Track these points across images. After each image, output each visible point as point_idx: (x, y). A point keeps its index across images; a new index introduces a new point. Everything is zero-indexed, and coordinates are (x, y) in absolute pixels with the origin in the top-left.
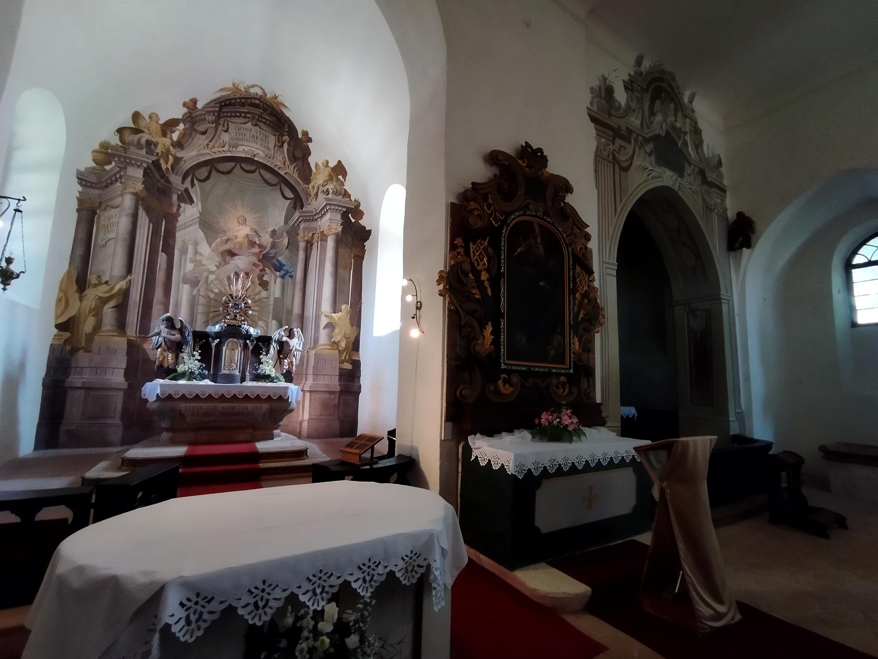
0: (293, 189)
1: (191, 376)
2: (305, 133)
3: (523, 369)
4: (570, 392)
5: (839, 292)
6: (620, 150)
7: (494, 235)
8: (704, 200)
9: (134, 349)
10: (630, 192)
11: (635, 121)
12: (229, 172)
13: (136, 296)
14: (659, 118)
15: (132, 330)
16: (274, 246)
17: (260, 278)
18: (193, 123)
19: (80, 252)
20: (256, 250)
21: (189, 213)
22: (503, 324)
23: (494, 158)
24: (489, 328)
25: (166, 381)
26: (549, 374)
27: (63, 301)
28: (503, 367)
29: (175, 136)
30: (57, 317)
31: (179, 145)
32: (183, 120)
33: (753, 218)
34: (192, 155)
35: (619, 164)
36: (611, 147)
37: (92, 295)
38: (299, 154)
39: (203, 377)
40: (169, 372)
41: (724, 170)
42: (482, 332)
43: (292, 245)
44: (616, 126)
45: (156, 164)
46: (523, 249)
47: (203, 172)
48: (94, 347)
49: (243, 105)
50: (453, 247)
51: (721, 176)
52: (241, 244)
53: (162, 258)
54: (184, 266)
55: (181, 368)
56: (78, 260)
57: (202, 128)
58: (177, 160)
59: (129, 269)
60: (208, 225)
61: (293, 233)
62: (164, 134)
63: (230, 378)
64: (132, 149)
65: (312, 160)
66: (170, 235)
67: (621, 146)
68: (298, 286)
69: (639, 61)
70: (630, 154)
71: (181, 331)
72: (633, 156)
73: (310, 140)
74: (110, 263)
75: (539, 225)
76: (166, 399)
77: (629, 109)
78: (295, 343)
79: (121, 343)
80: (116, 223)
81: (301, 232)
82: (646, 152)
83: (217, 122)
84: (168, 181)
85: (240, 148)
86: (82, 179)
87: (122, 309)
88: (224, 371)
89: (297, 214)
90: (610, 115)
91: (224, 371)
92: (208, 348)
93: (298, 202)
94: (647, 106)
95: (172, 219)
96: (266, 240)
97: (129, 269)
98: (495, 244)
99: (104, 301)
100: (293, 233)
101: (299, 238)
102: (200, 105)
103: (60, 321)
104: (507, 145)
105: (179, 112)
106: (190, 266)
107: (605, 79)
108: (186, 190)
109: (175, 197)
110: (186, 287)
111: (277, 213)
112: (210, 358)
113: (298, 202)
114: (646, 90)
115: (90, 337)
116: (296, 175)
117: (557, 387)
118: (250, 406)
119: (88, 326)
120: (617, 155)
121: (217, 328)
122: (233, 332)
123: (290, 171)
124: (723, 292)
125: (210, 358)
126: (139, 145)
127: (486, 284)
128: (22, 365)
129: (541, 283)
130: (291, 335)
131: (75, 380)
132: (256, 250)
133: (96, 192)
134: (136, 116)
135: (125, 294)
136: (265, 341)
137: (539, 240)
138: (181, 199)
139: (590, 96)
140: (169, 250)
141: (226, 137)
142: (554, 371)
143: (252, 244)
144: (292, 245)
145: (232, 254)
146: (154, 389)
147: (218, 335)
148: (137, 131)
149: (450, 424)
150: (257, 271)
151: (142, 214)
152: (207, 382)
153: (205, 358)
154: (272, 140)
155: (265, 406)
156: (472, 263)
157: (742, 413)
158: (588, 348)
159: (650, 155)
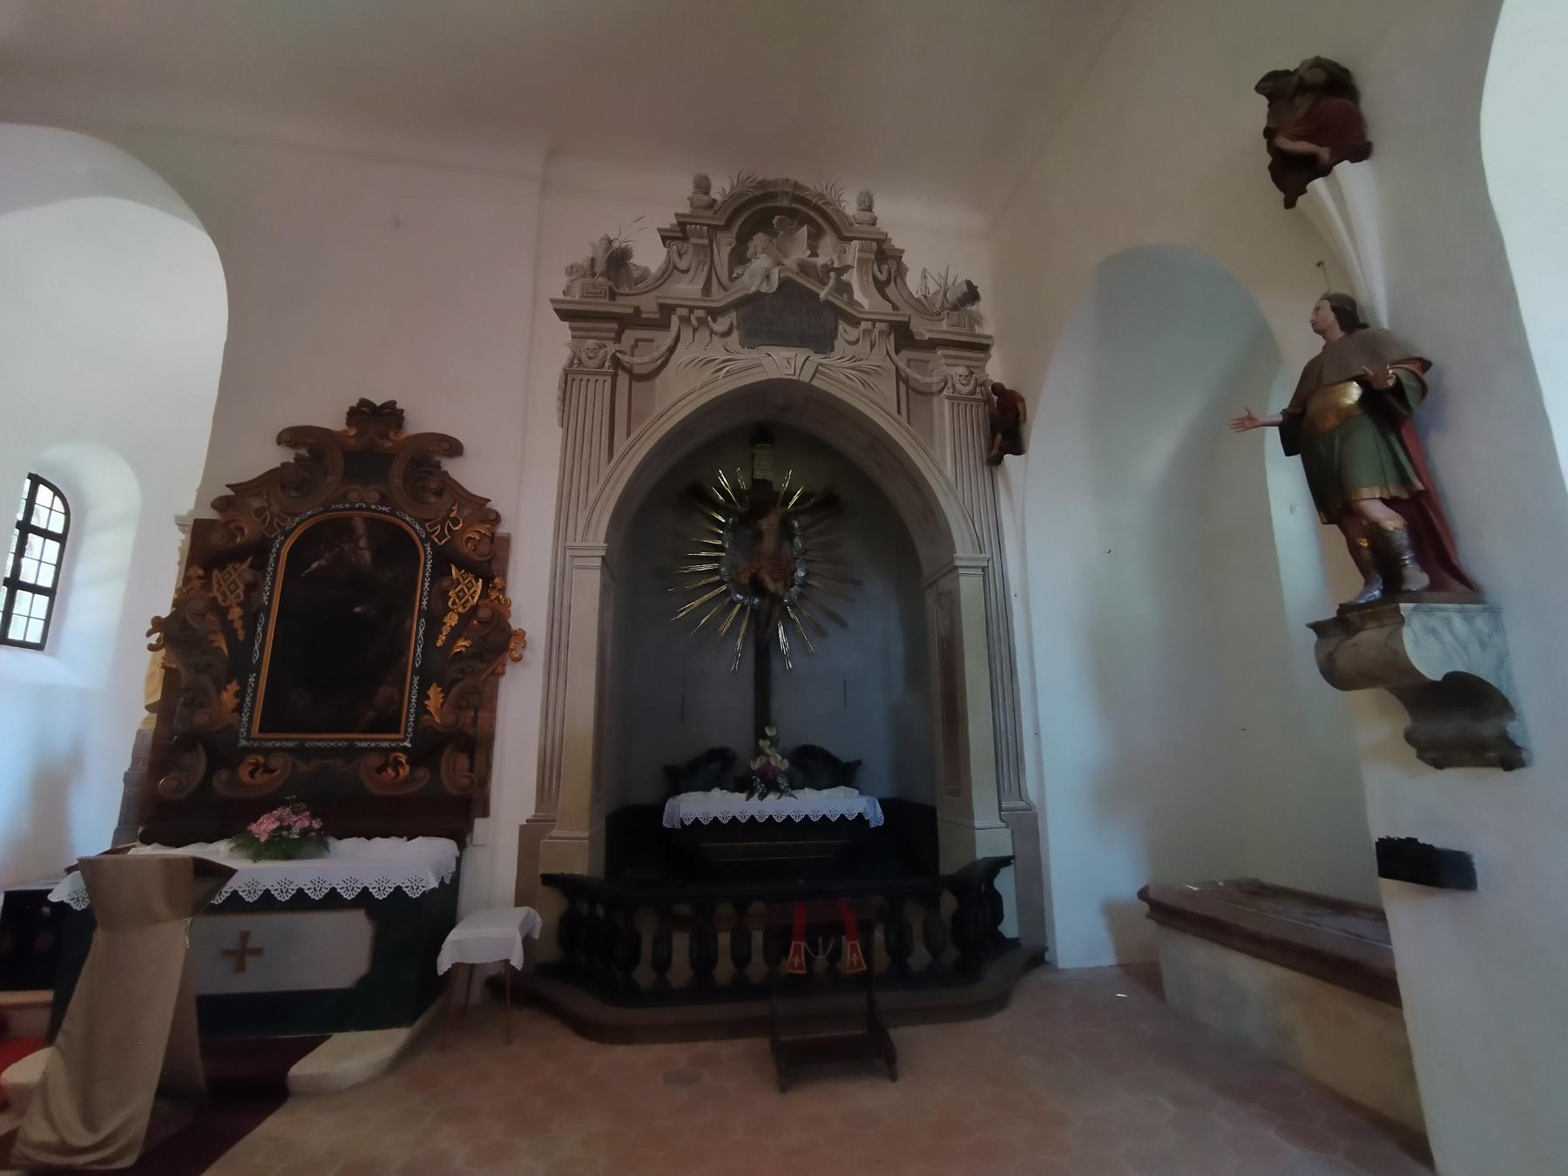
3: (291, 744)
4: (411, 778)
6: (635, 347)
7: (258, 552)
8: (900, 377)
10: (658, 410)
11: (687, 289)
14: (761, 262)
23: (292, 437)
24: (234, 687)
26: (352, 753)
28: (243, 743)
30: (148, 697)
33: (1024, 393)
35: (630, 372)
36: (611, 348)
41: (983, 307)
42: (219, 694)
44: (631, 311)
46: (323, 562)
51: (975, 320)
67: (637, 340)
69: (703, 185)
70: (664, 348)
72: (672, 349)
77: (670, 271)
82: (712, 332)
90: (613, 295)
94: (722, 255)
98: (260, 566)
103: (152, 701)
104: (328, 413)
107: (610, 242)
114: (727, 226)
117: (381, 769)
120: (625, 358)
124: (963, 550)
127: (238, 625)
129: (357, 610)
137: (362, 543)
142: (364, 744)
156: (215, 599)
157: (1030, 808)
158: (479, 702)
159: (728, 333)
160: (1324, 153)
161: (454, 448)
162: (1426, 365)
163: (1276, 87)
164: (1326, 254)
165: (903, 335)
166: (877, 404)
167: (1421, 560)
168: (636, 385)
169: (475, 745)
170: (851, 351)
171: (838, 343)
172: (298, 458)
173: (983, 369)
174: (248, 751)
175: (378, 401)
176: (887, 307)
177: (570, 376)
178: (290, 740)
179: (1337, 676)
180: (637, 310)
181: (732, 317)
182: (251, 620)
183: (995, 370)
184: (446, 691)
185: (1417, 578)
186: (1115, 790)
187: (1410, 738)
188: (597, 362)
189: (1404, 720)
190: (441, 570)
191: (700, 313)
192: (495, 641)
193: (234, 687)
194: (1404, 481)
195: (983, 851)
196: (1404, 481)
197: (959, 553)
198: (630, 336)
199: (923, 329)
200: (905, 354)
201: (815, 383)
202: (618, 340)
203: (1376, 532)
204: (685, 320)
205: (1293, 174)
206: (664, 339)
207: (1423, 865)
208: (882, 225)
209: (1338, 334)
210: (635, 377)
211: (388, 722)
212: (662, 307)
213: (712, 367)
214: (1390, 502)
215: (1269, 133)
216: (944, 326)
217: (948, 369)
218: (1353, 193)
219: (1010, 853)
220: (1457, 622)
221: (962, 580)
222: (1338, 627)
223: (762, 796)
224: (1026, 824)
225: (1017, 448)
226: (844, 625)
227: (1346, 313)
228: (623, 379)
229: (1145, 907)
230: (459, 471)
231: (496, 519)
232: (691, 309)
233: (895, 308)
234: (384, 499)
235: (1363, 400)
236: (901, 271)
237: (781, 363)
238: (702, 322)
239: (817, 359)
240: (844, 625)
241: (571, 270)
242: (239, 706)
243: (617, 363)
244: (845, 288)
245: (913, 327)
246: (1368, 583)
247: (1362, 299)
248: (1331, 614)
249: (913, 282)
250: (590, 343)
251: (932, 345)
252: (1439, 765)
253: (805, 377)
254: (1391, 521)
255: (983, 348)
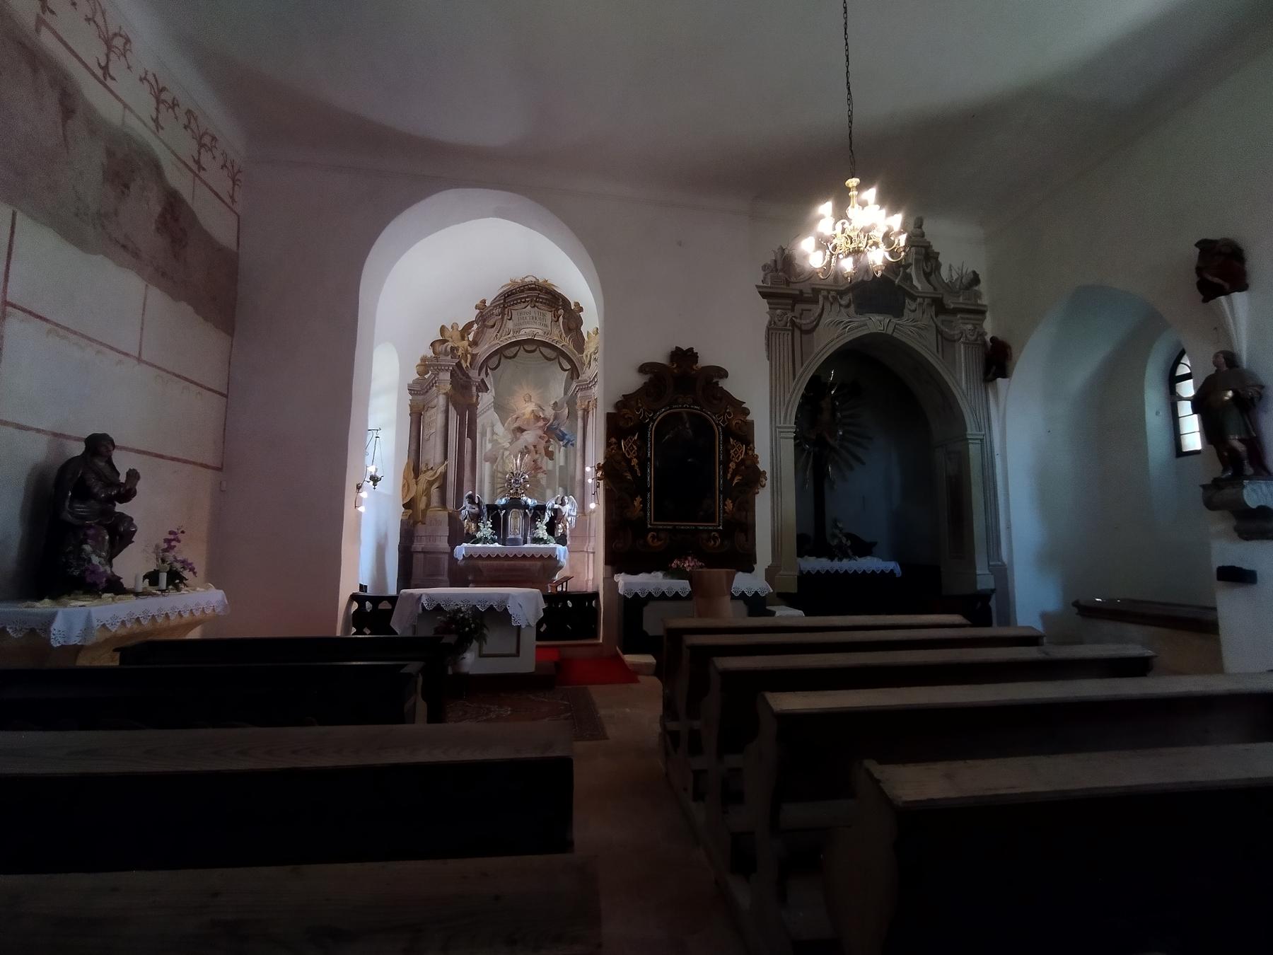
0: (570, 361)
1: (485, 540)
2: (577, 304)
5: (1157, 413)
7: (642, 428)
8: (939, 332)
9: (453, 520)
10: (816, 350)
12: (515, 355)
13: (451, 477)
15: (451, 506)
16: (556, 417)
17: (546, 449)
18: (484, 321)
19: (413, 447)
20: (541, 423)
21: (486, 399)
22: (651, 496)
24: (639, 499)
25: (469, 545)
27: (406, 487)
29: (471, 337)
31: (474, 343)
32: (476, 321)
34: (483, 350)
35: (800, 329)
36: (790, 315)
37: (424, 478)
38: (573, 325)
39: (494, 541)
40: (471, 538)
41: (982, 287)
43: (572, 415)
45: (459, 365)
47: (495, 359)
48: (428, 521)
49: (522, 291)
50: (608, 444)
51: (978, 295)
52: (528, 420)
53: (468, 442)
54: (485, 446)
55: (479, 535)
56: (413, 453)
57: (491, 323)
58: (474, 356)
59: (446, 458)
60: (501, 408)
61: (571, 403)
62: (463, 338)
63: (515, 542)
64: (442, 357)
65: (584, 329)
66: (473, 422)
68: (579, 454)
71: (479, 505)
72: (821, 315)
73: (581, 309)
74: (432, 453)
75: (688, 413)
76: (469, 558)
78: (567, 509)
79: (444, 516)
80: (435, 419)
81: (578, 402)
83: (502, 314)
84: (468, 377)
85: (522, 332)
86: (412, 390)
87: (443, 489)
88: (510, 536)
89: (574, 385)
91: (510, 536)
92: (497, 516)
93: (574, 372)
95: (472, 408)
96: (549, 413)
97: (446, 458)
98: (643, 438)
99: (431, 483)
100: (571, 403)
101: (577, 407)
102: (488, 304)
105: (472, 315)
106: (489, 446)
108: (483, 380)
109: (474, 389)
110: (487, 465)
111: (557, 387)
112: (499, 526)
113: (574, 372)
115: (424, 512)
116: (571, 346)
118: (527, 563)
119: (422, 505)
121: (503, 501)
122: (515, 503)
123: (565, 343)
124: (971, 430)
125: (499, 526)
126: (446, 354)
127: (636, 468)
128: (386, 535)
130: (563, 504)
131: (418, 546)
132: (541, 423)
133: (421, 397)
134: (443, 329)
135: (444, 476)
136: (540, 510)
138: (479, 390)
139: (762, 273)
140: (472, 435)
141: (510, 325)
143: (538, 418)
144: (572, 415)
145: (521, 430)
146: (462, 550)
147: (504, 507)
148: (444, 341)
149: (609, 568)
150: (543, 443)
151: (451, 407)
152: (497, 545)
153: (495, 527)
154: (549, 316)
155: (539, 563)
157: (1004, 565)
158: (747, 507)
159: (848, 306)
160: (1227, 286)
161: (722, 373)
162: (1262, 387)
163: (1206, 247)
164: (1220, 328)
165: (939, 306)
166: (926, 347)
167: (1251, 463)
168: (805, 337)
169: (747, 529)
170: (912, 315)
171: (906, 311)
172: (651, 380)
173: (981, 326)
174: (651, 530)
175: (685, 348)
176: (930, 289)
177: (771, 330)
178: (669, 525)
179: (1210, 505)
180: (801, 291)
181: (850, 296)
182: (643, 463)
183: (990, 328)
184: (733, 503)
185: (1249, 470)
186: (1050, 557)
187: (1236, 529)
188: (783, 323)
189: (1233, 522)
190: (726, 441)
191: (833, 293)
192: (752, 478)
193: (639, 499)
194: (1248, 432)
195: (980, 587)
196: (1248, 432)
197: (969, 432)
198: (798, 307)
199: (950, 303)
200: (942, 317)
201: (895, 335)
202: (793, 310)
203: (1233, 451)
204: (826, 298)
205: (1209, 291)
206: (816, 310)
207: (1237, 576)
208: (927, 238)
209: (1225, 368)
210: (803, 332)
211: (710, 517)
212: (814, 290)
213: (841, 326)
214: (1240, 440)
215: (1199, 270)
216: (961, 300)
217: (964, 326)
218: (1239, 306)
219: (992, 587)
220: (1264, 487)
221: (971, 446)
222: (1217, 484)
223: (840, 560)
224: (1002, 573)
225: (1003, 372)
226: (863, 463)
227: (1230, 359)
228: (797, 333)
229: (1076, 610)
230: (727, 385)
231: (746, 412)
232: (829, 291)
233: (935, 289)
234: (695, 402)
235: (1233, 399)
236: (938, 266)
237: (876, 323)
238: (835, 298)
239: (894, 320)
240: (863, 463)
241: (765, 267)
242: (643, 506)
243: (793, 323)
244: (908, 277)
245: (945, 301)
246: (1225, 470)
247: (1236, 350)
248: (1208, 481)
249: (944, 273)
250: (778, 312)
251: (955, 311)
252: (1247, 539)
253: (890, 332)
254: (1240, 447)
255: (981, 312)
